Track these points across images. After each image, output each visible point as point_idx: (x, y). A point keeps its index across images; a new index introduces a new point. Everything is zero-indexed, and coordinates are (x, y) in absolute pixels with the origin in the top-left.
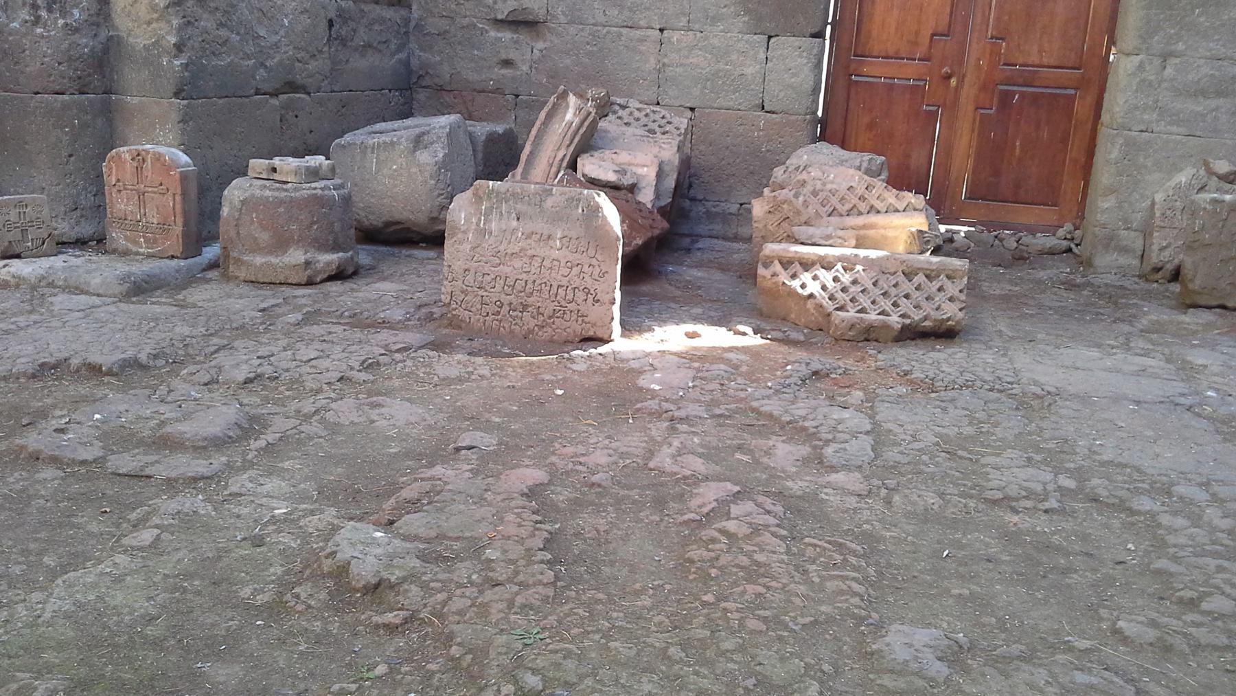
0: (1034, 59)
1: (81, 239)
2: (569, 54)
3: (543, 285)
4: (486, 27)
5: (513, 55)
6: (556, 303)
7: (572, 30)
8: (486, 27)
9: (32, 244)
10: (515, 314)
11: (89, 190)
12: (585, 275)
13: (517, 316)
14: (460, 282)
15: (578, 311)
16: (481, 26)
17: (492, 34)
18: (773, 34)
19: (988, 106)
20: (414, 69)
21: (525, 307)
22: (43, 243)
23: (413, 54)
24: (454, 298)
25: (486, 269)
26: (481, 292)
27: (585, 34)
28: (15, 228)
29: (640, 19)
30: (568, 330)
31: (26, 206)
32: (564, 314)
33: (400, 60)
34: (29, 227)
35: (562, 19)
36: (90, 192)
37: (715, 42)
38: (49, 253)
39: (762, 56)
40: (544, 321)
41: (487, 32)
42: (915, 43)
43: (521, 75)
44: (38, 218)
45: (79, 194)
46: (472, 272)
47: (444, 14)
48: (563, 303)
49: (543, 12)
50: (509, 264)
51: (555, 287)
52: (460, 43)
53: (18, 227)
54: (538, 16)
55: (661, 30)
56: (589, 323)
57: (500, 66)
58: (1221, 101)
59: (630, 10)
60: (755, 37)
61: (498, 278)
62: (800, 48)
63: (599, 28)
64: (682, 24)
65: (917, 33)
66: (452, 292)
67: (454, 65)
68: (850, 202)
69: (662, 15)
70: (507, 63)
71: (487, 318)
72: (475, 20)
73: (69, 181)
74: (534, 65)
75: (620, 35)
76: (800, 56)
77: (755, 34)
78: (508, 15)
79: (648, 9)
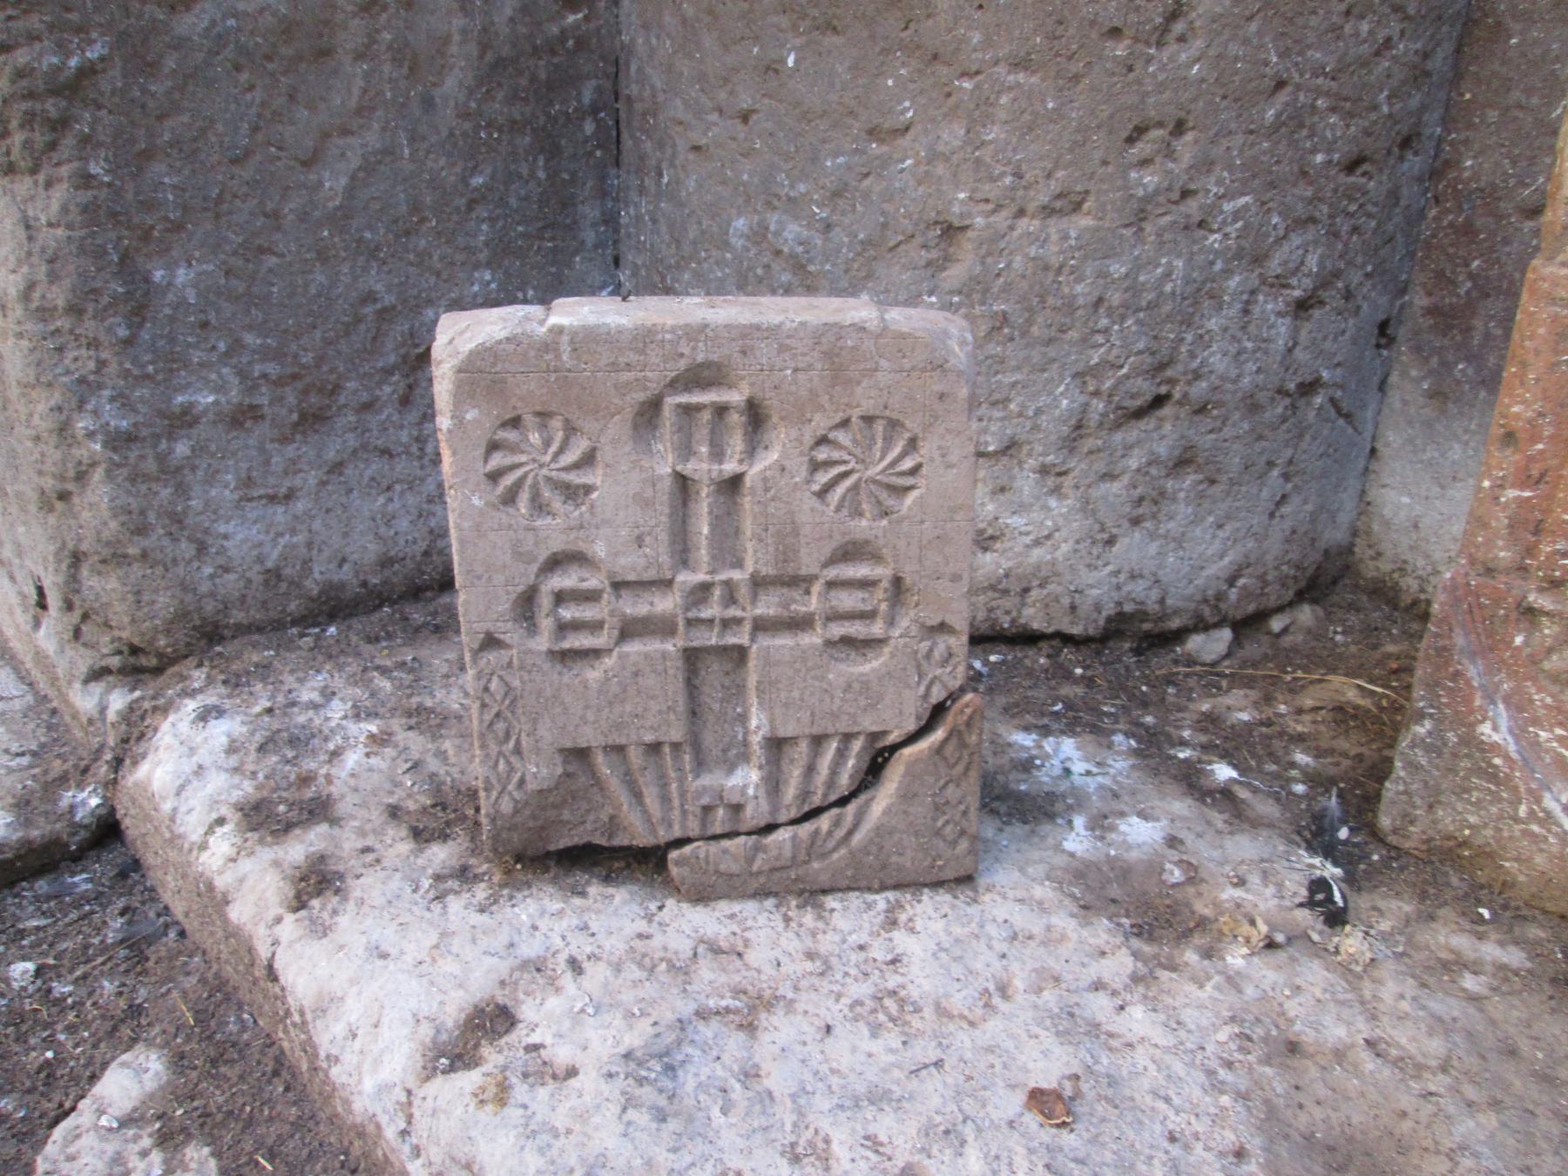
1: (1142, 615)
9: (773, 784)
11: (1274, 266)
22: (874, 769)
28: (629, 630)
31: (756, 416)
34: (761, 626)
36: (1280, 283)
38: (908, 860)
44: (850, 552)
45: (1202, 293)
53: (662, 627)
73: (1150, 179)
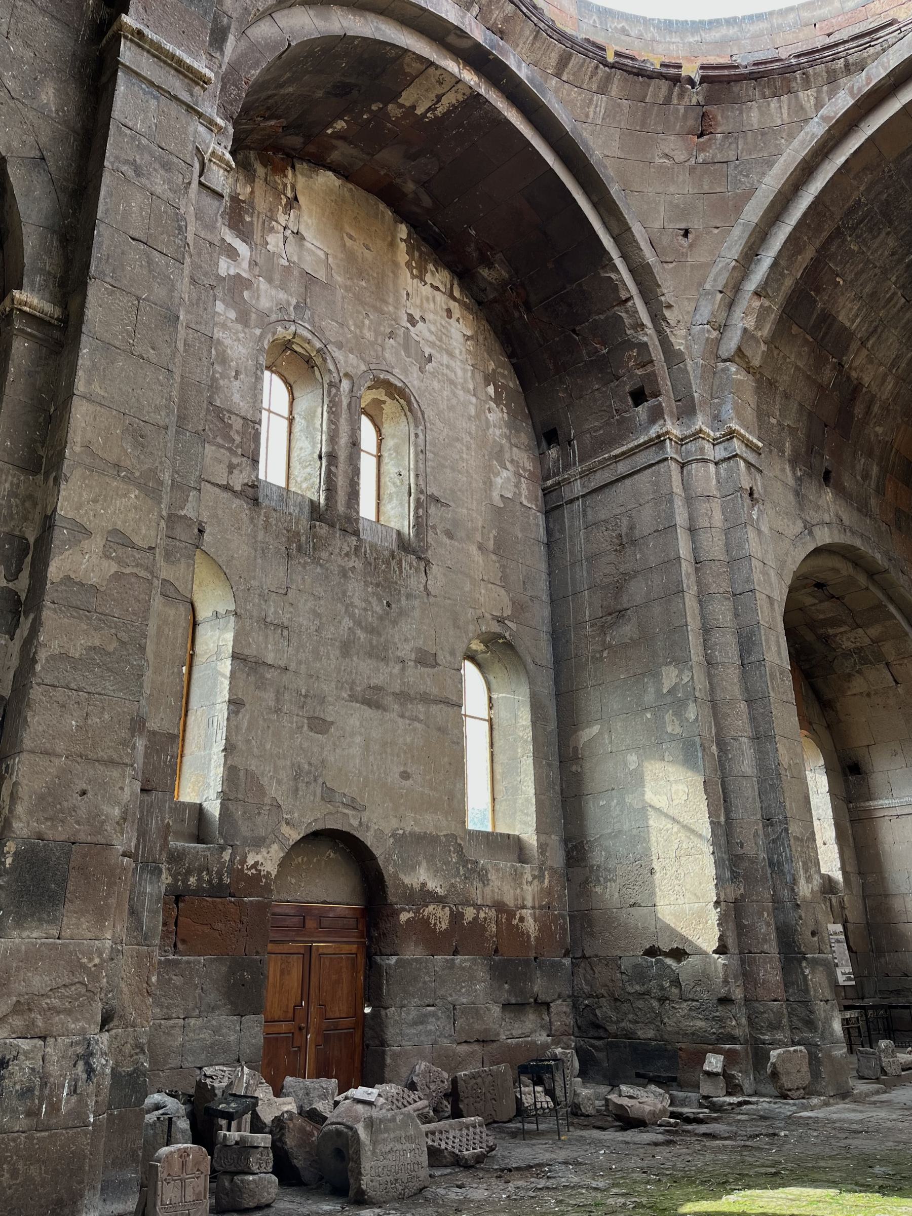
0: (337, 1015)
21: (396, 1180)
26: (378, 1179)
37: (214, 1023)
39: (238, 1028)
42: (286, 1012)
55: (184, 1019)
58: (421, 1027)
59: (167, 1008)
60: (235, 1018)
65: (287, 1006)
69: (185, 1009)
75: (160, 1025)
79: (177, 1006)
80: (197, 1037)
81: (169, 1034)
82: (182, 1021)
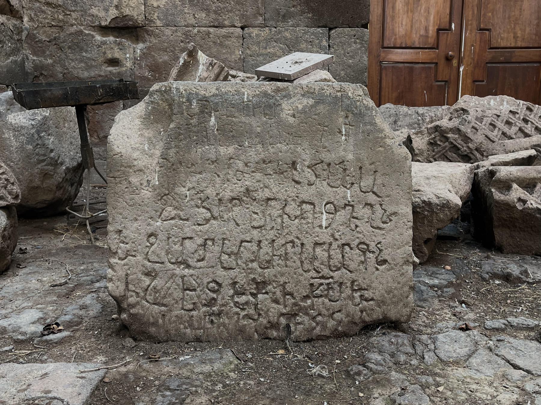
2: (167, 52)
3: (289, 246)
4: (92, 33)
5: (117, 54)
6: (313, 274)
7: (168, 32)
8: (92, 33)
10: (243, 299)
12: (358, 222)
13: (247, 303)
14: (139, 258)
15: (353, 282)
16: (87, 32)
17: (98, 38)
18: (332, 26)
19: (481, 79)
20: (29, 71)
23: (28, 59)
24: (131, 287)
25: (186, 230)
26: (179, 270)
27: (179, 34)
29: (225, 20)
30: (337, 316)
32: (328, 289)
33: (16, 61)
35: (158, 23)
37: (287, 34)
39: (325, 43)
40: (295, 304)
41: (93, 37)
43: (126, 70)
46: (162, 236)
47: (53, 23)
48: (326, 271)
49: (141, 18)
50: (226, 217)
51: (309, 247)
52: (69, 48)
54: (136, 21)
56: (372, 299)
57: (107, 65)
59: (215, 12)
60: (319, 29)
61: (209, 243)
62: (355, 36)
63: (190, 29)
64: (259, 22)
66: (127, 275)
67: (65, 66)
68: (516, 125)
69: (242, 16)
70: (114, 62)
71: (194, 313)
72: (82, 28)
74: (137, 62)
75: (209, 33)
76: (355, 43)
77: (319, 27)
78: (110, 22)
79: (231, 11)
80: (264, 51)
81: (221, 45)
82: (239, 30)
